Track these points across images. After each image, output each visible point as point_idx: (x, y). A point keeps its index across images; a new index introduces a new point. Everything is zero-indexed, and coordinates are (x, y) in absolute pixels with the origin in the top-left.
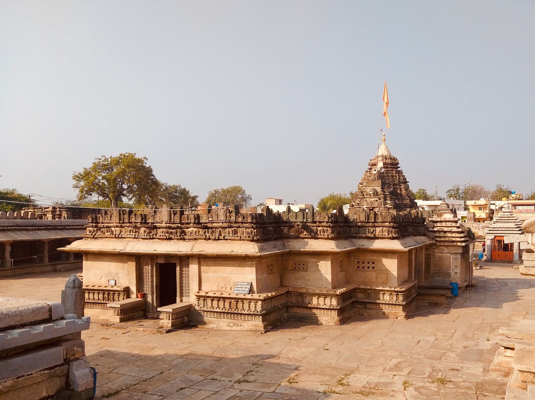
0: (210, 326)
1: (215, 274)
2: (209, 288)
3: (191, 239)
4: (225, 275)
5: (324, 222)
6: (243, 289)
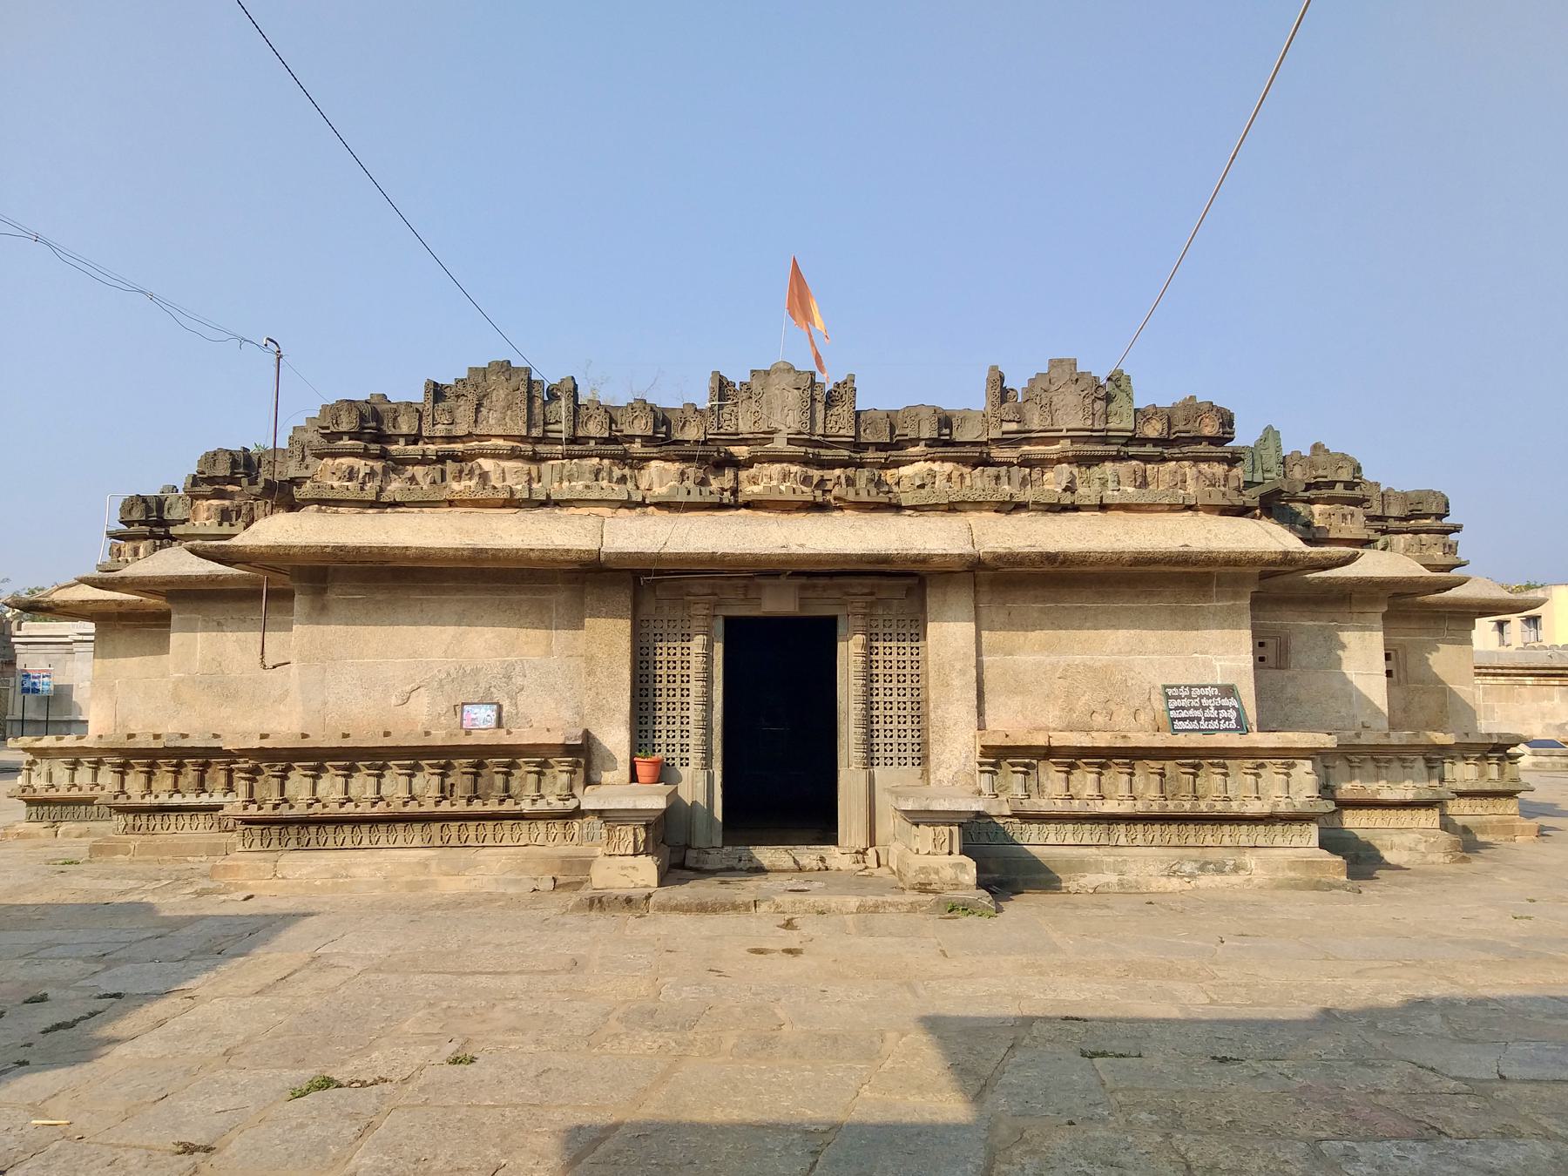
0: (1091, 879)
1: (1054, 659)
2: (1012, 721)
3: (934, 508)
4: (1101, 660)
5: (1331, 485)
6: (1212, 713)
